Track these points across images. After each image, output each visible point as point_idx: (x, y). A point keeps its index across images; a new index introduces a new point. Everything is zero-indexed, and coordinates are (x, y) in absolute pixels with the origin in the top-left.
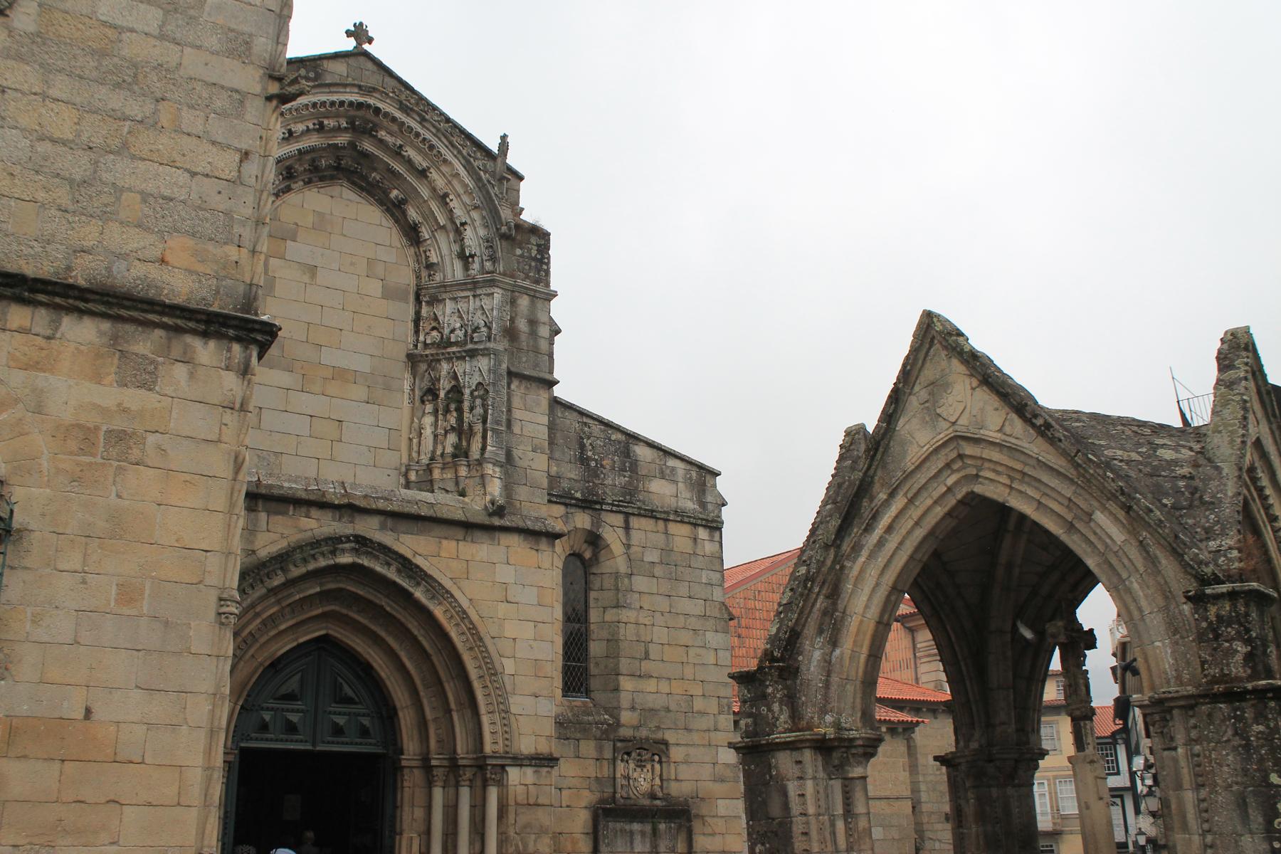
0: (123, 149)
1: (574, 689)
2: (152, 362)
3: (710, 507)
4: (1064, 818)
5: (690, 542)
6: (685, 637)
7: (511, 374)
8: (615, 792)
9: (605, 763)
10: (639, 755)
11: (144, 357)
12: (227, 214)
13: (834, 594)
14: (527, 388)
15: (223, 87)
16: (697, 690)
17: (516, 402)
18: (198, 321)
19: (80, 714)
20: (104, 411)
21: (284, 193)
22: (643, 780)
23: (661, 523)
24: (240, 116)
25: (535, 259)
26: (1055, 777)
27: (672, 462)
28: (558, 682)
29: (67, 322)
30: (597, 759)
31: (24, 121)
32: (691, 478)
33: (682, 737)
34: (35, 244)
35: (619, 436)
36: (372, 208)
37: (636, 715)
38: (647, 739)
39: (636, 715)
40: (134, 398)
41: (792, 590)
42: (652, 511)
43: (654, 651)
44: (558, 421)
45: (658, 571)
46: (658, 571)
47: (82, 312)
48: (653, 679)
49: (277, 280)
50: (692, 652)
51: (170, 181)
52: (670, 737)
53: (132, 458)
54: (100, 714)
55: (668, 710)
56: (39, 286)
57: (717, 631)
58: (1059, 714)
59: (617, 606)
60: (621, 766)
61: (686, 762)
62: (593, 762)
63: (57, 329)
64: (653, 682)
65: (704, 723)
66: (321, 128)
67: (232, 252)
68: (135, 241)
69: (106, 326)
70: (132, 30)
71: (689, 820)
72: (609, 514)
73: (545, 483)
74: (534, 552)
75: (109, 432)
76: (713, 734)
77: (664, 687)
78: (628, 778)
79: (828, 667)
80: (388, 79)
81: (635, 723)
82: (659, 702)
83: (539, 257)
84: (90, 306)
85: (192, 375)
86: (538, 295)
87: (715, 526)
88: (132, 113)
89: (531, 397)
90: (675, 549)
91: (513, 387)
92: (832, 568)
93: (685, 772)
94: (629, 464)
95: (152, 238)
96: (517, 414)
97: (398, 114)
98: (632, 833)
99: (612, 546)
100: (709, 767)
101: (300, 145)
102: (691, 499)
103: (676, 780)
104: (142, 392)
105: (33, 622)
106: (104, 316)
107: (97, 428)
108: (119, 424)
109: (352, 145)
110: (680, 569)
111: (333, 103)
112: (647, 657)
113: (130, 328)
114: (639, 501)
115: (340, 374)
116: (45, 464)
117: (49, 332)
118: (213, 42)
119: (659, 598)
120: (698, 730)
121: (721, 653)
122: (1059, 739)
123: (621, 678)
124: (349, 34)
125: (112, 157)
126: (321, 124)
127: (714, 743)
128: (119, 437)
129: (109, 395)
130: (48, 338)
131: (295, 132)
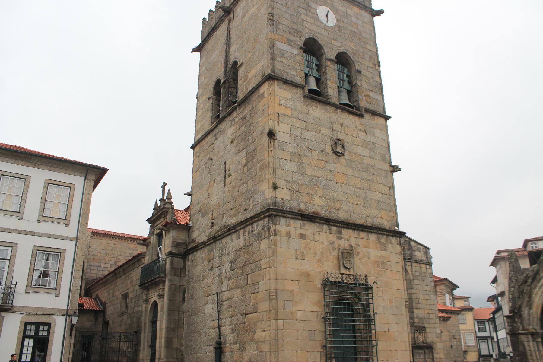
0: (369, 189)
2: (385, 244)
3: (429, 259)
4: (468, 346)
5: (425, 269)
6: (427, 297)
8: (415, 342)
9: (412, 333)
10: (420, 331)
13: (530, 297)
15: (383, 170)
16: (430, 312)
18: (392, 233)
19: (387, 330)
23: (419, 264)
26: (465, 333)
27: (420, 246)
29: (370, 235)
31: (352, 184)
34: (359, 215)
38: (421, 326)
40: (384, 253)
41: (511, 294)
42: (417, 261)
45: (419, 278)
46: (419, 278)
47: (372, 232)
50: (429, 301)
51: (379, 196)
52: (426, 325)
53: (386, 268)
54: (390, 330)
55: (425, 318)
56: (366, 227)
58: (466, 311)
59: (411, 289)
60: (416, 334)
61: (430, 333)
63: (368, 237)
64: (421, 310)
68: (376, 213)
69: (376, 235)
70: (365, 156)
71: (432, 349)
75: (381, 262)
78: (417, 337)
79: (529, 314)
81: (418, 322)
84: (374, 231)
85: (392, 246)
87: (430, 264)
88: (369, 179)
92: (529, 291)
93: (430, 335)
94: (411, 248)
95: (379, 212)
99: (409, 272)
104: (385, 251)
105: (377, 309)
106: (376, 233)
107: (379, 261)
108: (382, 260)
112: (419, 303)
113: (380, 236)
116: (372, 271)
117: (367, 238)
118: (379, 157)
122: (466, 320)
125: (368, 191)
128: (383, 263)
129: (380, 253)
130: (368, 239)
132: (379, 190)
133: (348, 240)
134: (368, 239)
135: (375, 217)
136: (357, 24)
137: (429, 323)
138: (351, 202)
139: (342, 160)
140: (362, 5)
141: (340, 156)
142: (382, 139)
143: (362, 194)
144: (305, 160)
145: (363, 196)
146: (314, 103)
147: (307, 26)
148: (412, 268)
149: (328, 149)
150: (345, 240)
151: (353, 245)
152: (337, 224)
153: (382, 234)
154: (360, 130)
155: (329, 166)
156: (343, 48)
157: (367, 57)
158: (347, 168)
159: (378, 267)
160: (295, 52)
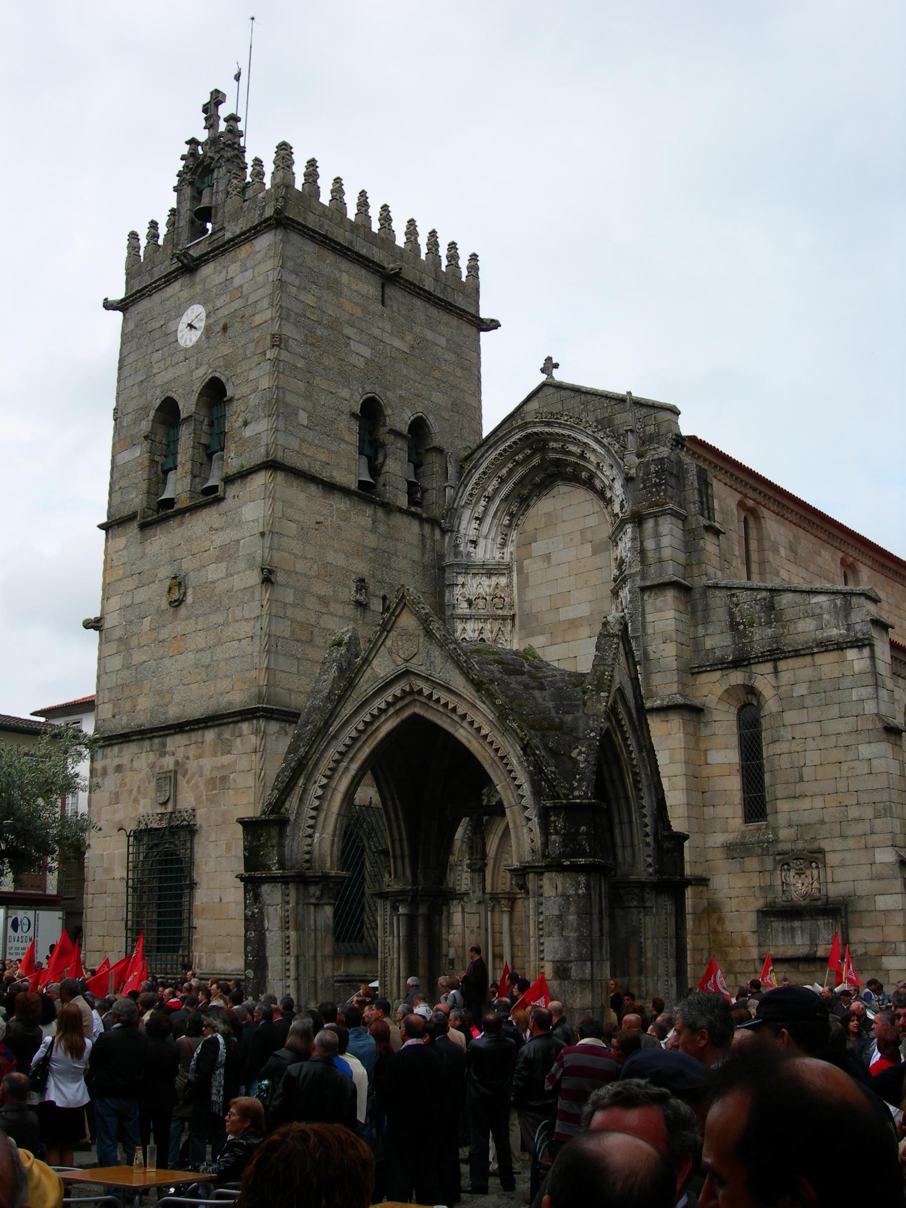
1: (756, 815)
2: (230, 740)
3: (858, 627)
6: (836, 755)
7: (643, 589)
11: (228, 739)
12: (252, 654)
14: (656, 594)
17: (648, 608)
19: (218, 900)
20: (218, 768)
21: (525, 511)
22: (800, 885)
23: (808, 659)
24: (253, 600)
25: (657, 485)
28: (739, 811)
30: (760, 872)
32: (836, 605)
33: (838, 844)
35: (764, 594)
36: (578, 490)
37: (793, 831)
39: (793, 831)
40: (226, 759)
43: (808, 773)
44: (710, 602)
45: (808, 702)
48: (806, 798)
49: (530, 574)
50: (844, 767)
52: (826, 845)
53: (227, 787)
55: (822, 822)
57: (870, 742)
61: (843, 866)
62: (756, 874)
65: (860, 828)
66: (518, 464)
67: (254, 674)
69: (217, 729)
72: (759, 665)
73: (674, 665)
74: (665, 723)
76: (868, 838)
77: (818, 802)
80: (563, 393)
81: (793, 838)
82: (812, 817)
83: (658, 481)
86: (658, 514)
89: (659, 602)
90: (823, 677)
91: (646, 597)
93: (840, 875)
95: (229, 680)
96: (649, 618)
97: (547, 430)
98: (793, 929)
100: (866, 869)
101: (514, 480)
102: (837, 626)
103: (833, 882)
108: (223, 773)
109: (543, 459)
110: (828, 694)
111: (510, 446)
113: (223, 728)
114: (784, 645)
115: (573, 624)
118: (242, 565)
119: (809, 725)
120: (853, 836)
121: (875, 762)
123: (778, 802)
124: (543, 371)
126: (515, 460)
127: (870, 845)
128: (224, 779)
131: (503, 476)
132: (235, 635)
133: (174, 754)
134: (203, 742)
135: (221, 694)
136: (241, 286)
137: (843, 836)
138: (187, 683)
139: (183, 611)
140: (249, 231)
141: (178, 606)
142: (253, 521)
143: (206, 659)
144: (134, 643)
145: (207, 661)
146: (152, 532)
147: (159, 383)
148: (777, 678)
149: (164, 604)
150: (169, 756)
151: (180, 761)
152: (156, 734)
153: (221, 725)
154: (217, 530)
155: (164, 634)
156: (211, 370)
157: (251, 346)
158: (187, 622)
159: (214, 789)
160: (137, 452)
